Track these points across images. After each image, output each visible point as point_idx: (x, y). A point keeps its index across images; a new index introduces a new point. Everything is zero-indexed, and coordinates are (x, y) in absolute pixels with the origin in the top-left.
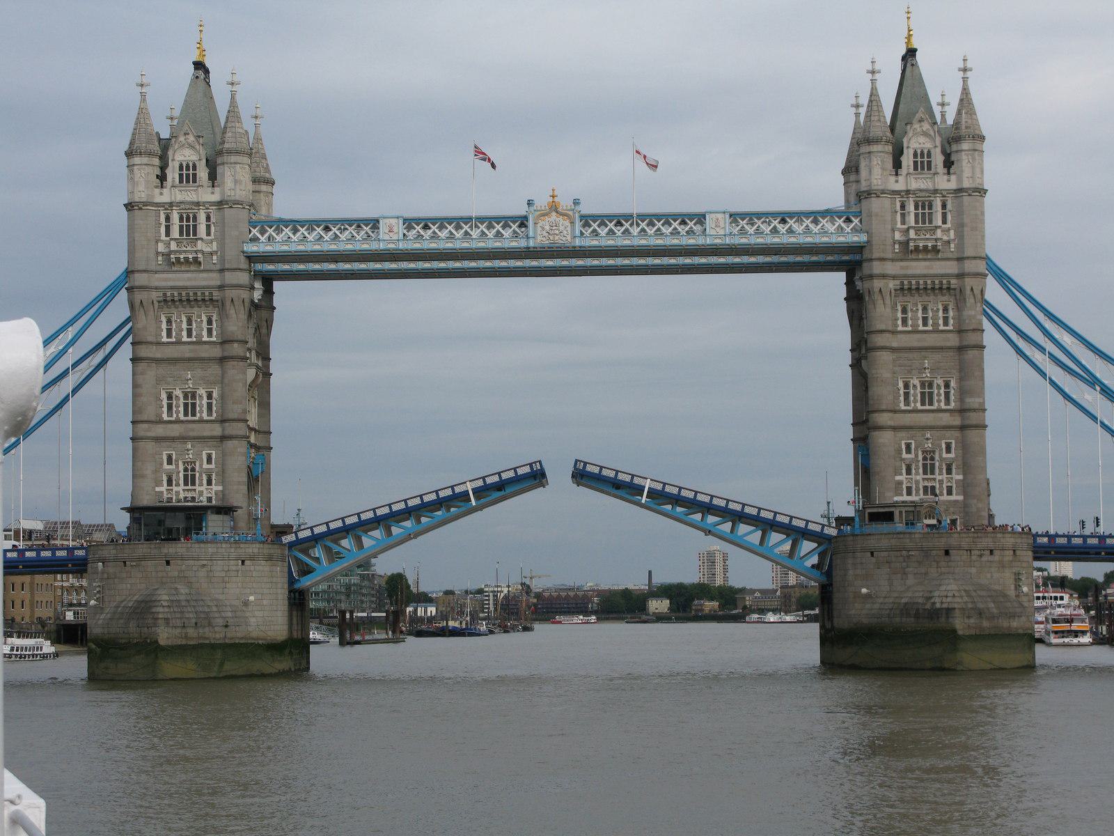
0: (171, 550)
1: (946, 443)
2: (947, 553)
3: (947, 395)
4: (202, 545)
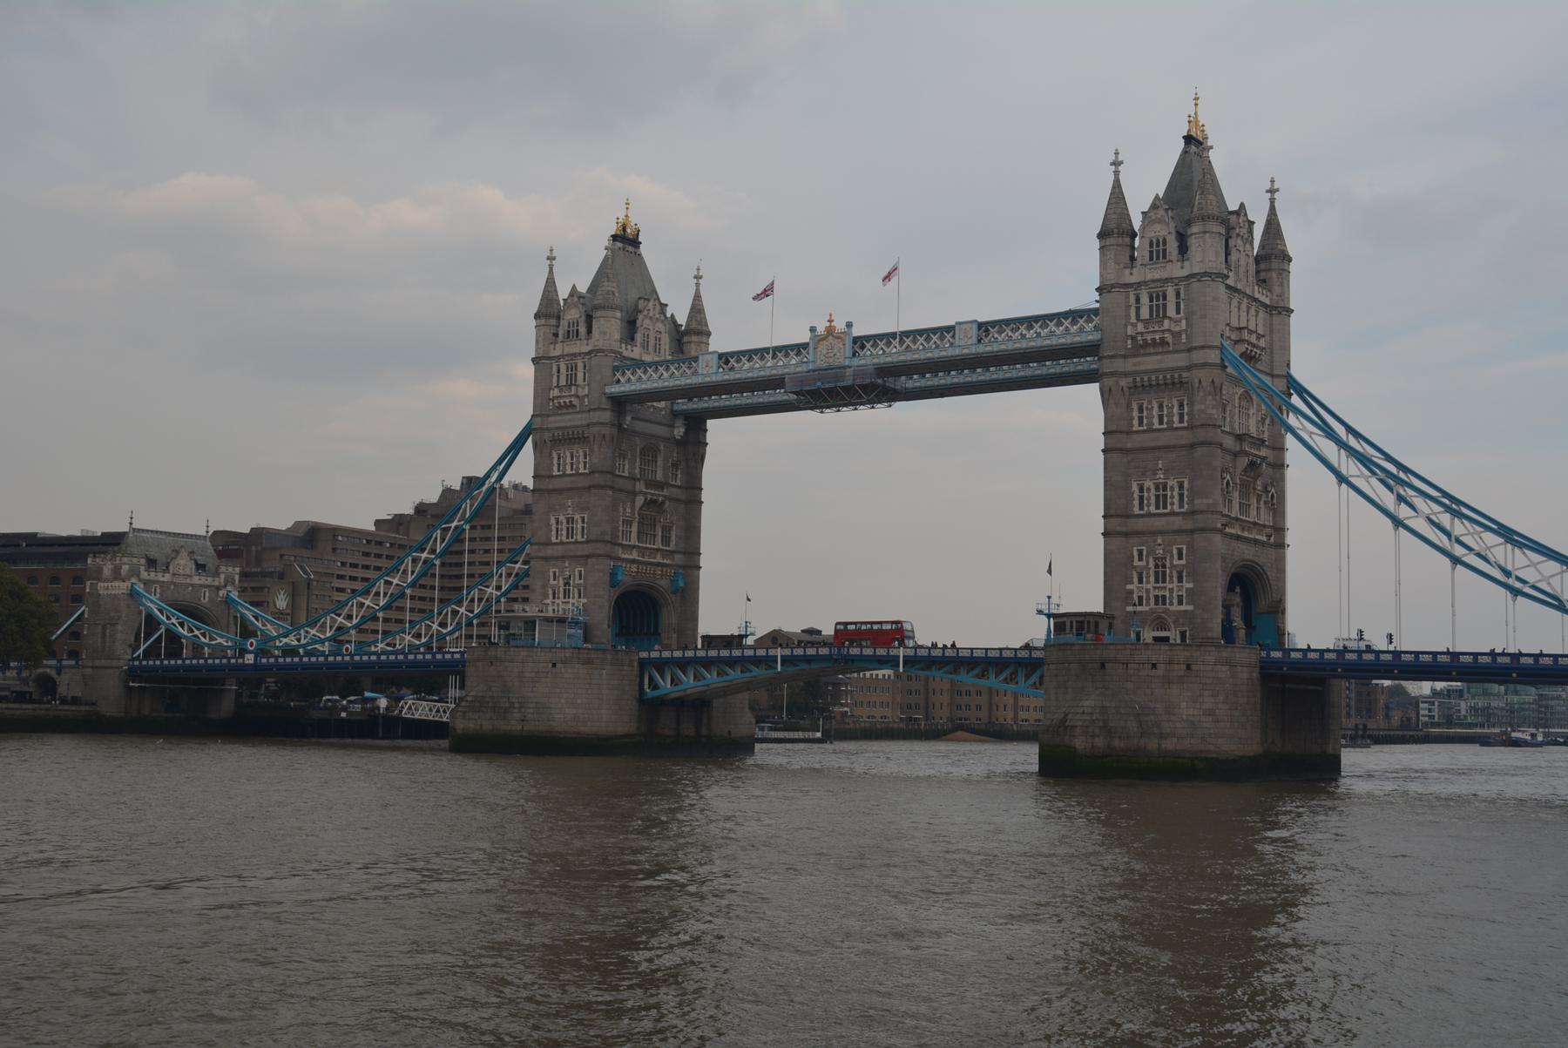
0: (493, 653)
1: (1177, 548)
2: (1103, 665)
3: (1181, 496)
4: (516, 649)
